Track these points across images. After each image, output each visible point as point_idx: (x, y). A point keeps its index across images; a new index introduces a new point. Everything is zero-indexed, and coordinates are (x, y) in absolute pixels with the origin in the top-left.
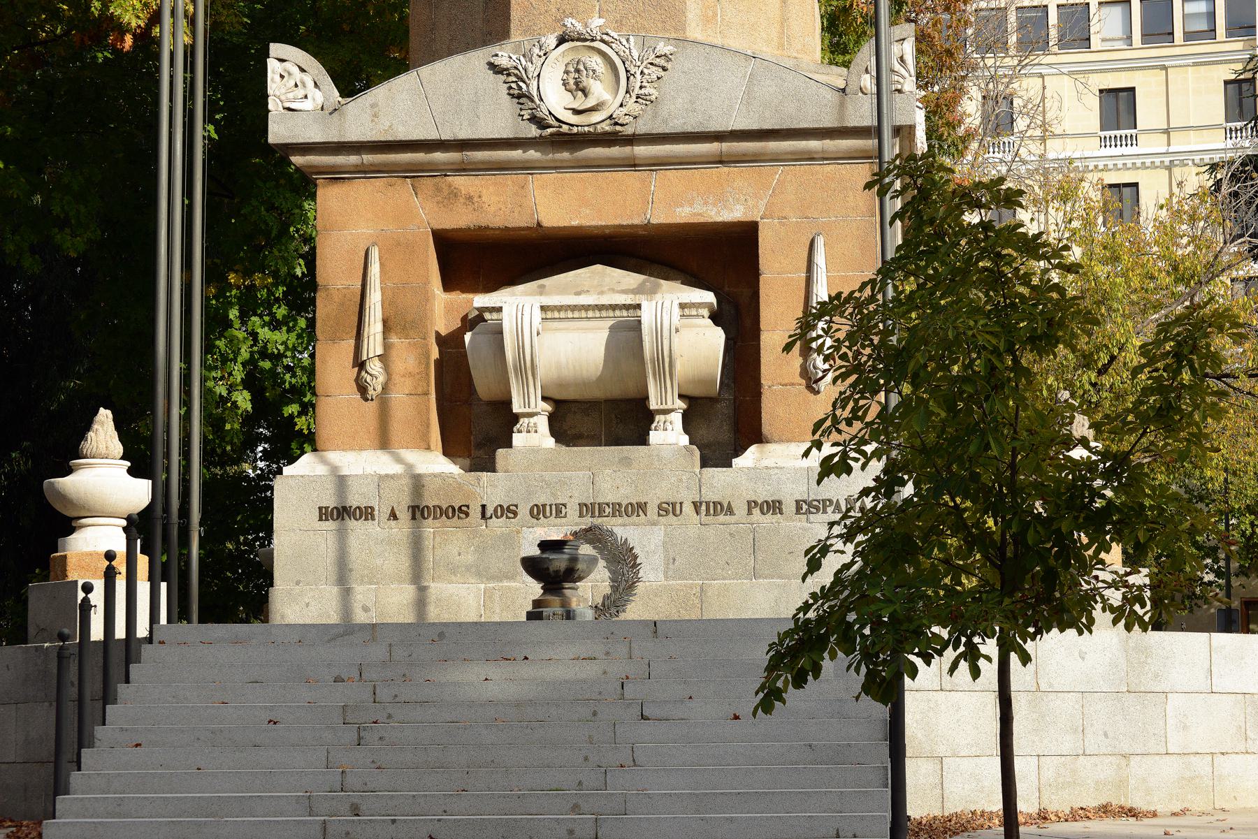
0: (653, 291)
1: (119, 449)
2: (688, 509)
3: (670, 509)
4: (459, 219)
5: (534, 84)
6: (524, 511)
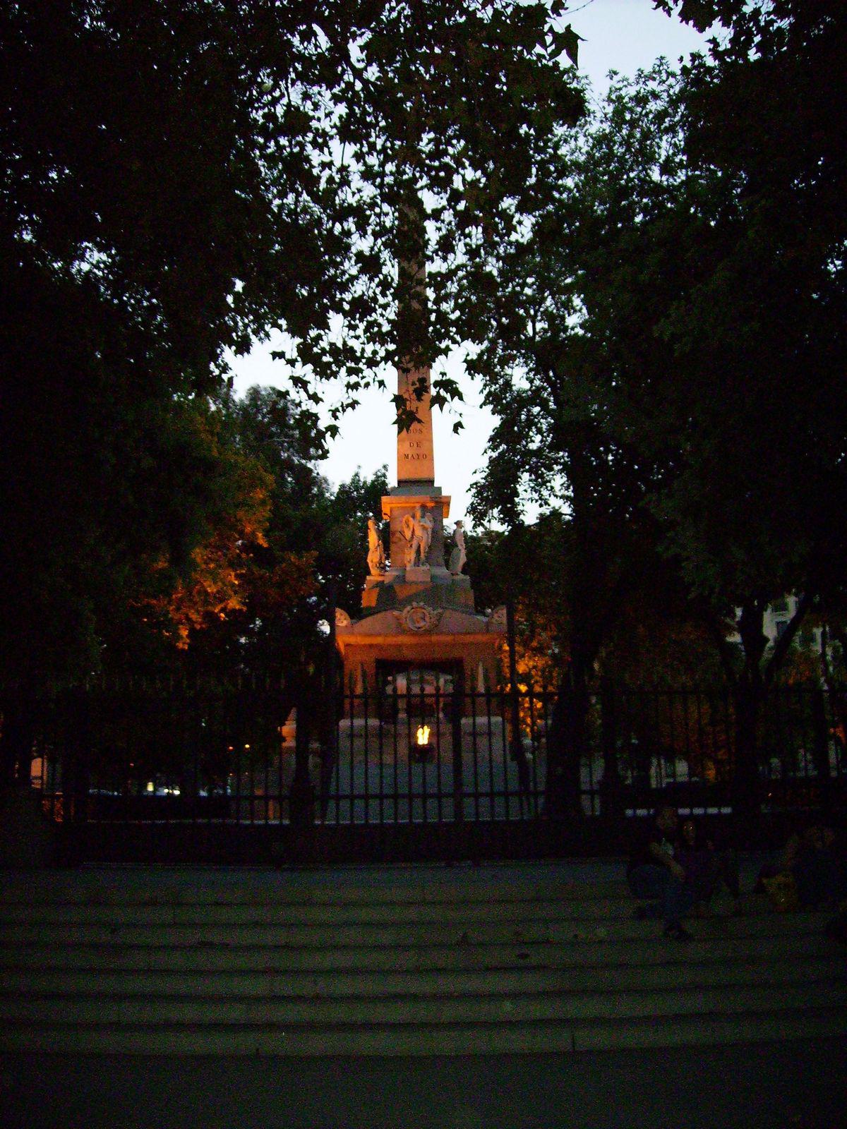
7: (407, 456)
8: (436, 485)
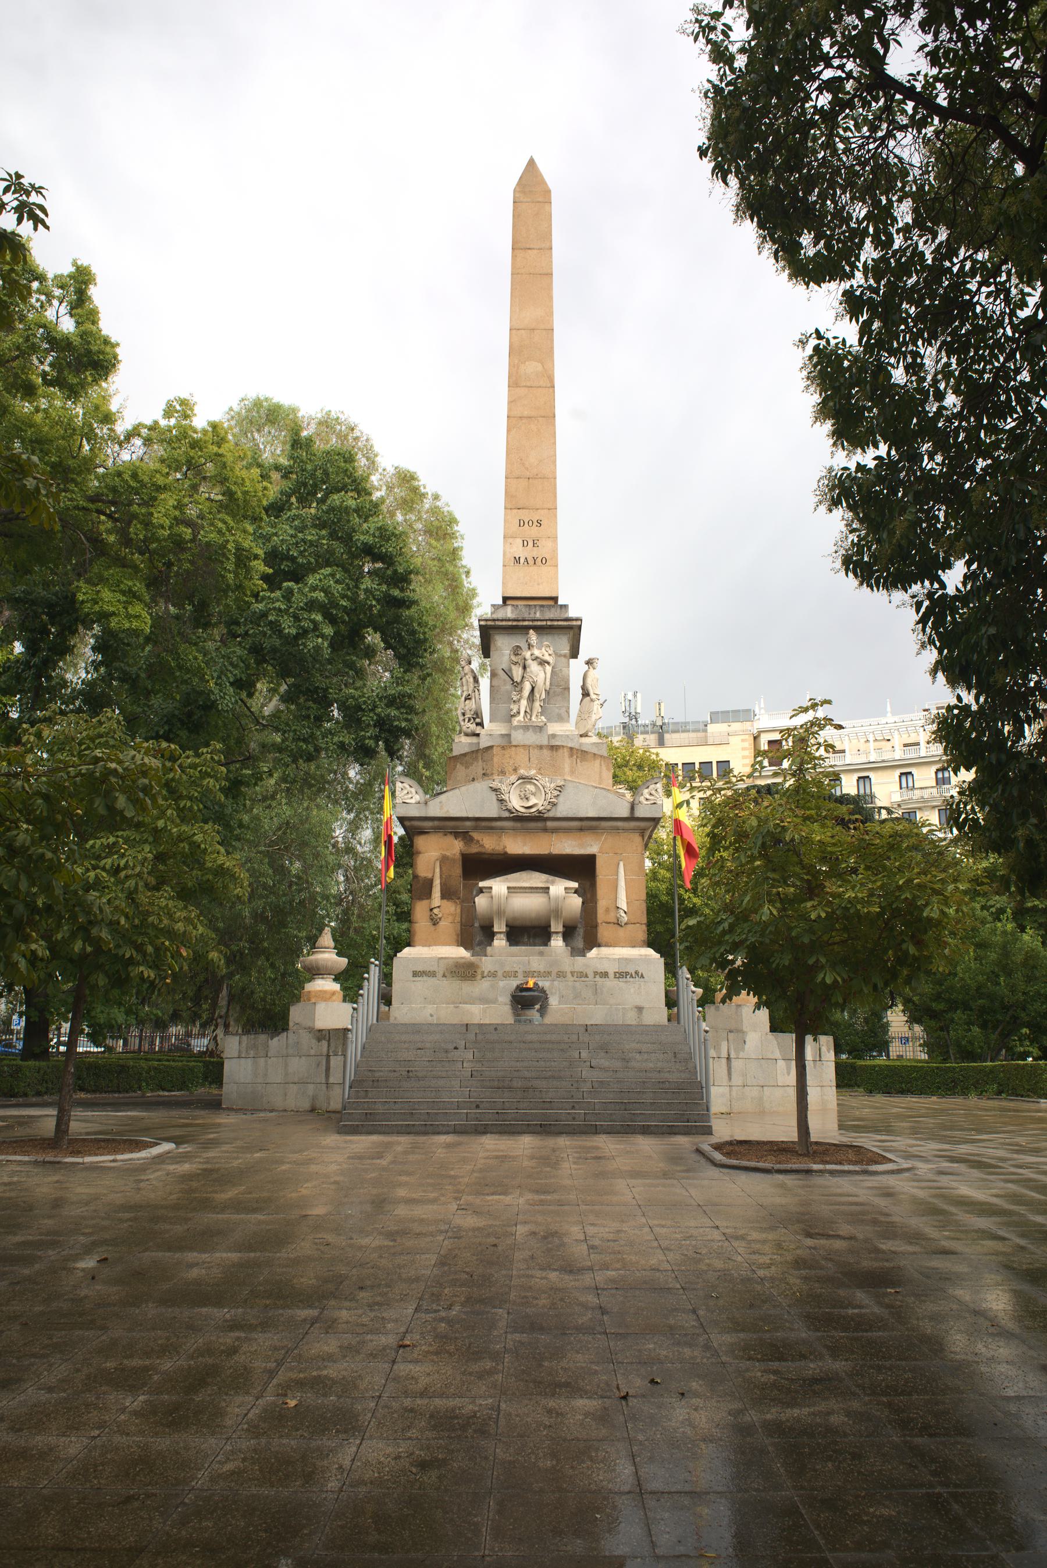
0: (553, 883)
1: (332, 944)
2: (569, 975)
3: (561, 975)
4: (474, 849)
6: (500, 974)
7: (517, 560)
8: (560, 602)
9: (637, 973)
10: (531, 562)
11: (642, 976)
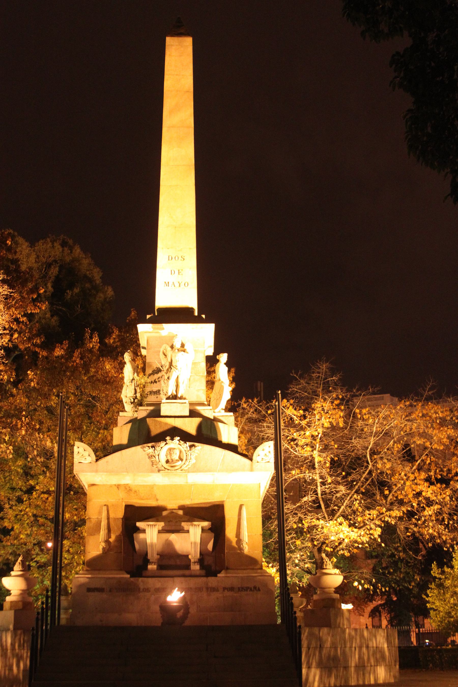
2: (204, 589)
5: (157, 457)
9: (255, 588)
10: (177, 285)
11: (259, 590)
